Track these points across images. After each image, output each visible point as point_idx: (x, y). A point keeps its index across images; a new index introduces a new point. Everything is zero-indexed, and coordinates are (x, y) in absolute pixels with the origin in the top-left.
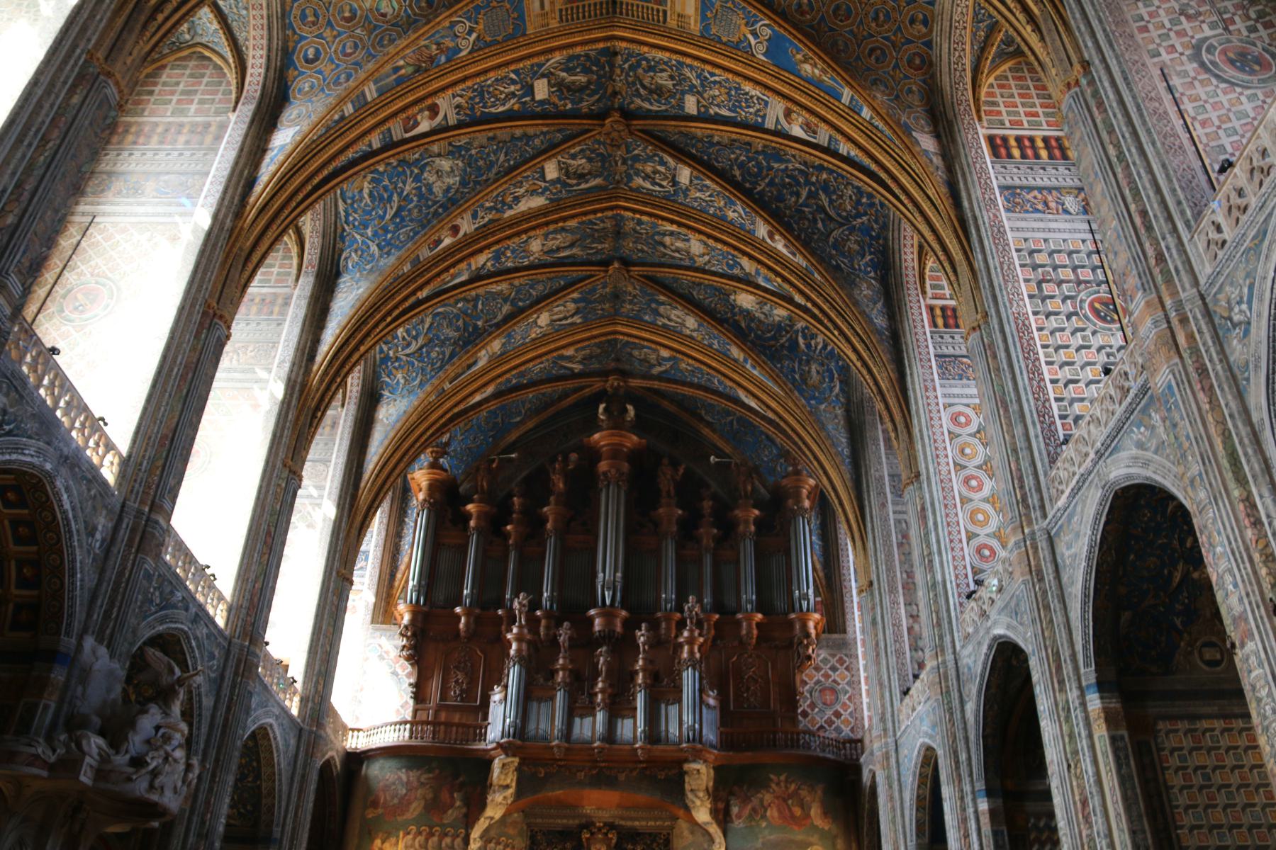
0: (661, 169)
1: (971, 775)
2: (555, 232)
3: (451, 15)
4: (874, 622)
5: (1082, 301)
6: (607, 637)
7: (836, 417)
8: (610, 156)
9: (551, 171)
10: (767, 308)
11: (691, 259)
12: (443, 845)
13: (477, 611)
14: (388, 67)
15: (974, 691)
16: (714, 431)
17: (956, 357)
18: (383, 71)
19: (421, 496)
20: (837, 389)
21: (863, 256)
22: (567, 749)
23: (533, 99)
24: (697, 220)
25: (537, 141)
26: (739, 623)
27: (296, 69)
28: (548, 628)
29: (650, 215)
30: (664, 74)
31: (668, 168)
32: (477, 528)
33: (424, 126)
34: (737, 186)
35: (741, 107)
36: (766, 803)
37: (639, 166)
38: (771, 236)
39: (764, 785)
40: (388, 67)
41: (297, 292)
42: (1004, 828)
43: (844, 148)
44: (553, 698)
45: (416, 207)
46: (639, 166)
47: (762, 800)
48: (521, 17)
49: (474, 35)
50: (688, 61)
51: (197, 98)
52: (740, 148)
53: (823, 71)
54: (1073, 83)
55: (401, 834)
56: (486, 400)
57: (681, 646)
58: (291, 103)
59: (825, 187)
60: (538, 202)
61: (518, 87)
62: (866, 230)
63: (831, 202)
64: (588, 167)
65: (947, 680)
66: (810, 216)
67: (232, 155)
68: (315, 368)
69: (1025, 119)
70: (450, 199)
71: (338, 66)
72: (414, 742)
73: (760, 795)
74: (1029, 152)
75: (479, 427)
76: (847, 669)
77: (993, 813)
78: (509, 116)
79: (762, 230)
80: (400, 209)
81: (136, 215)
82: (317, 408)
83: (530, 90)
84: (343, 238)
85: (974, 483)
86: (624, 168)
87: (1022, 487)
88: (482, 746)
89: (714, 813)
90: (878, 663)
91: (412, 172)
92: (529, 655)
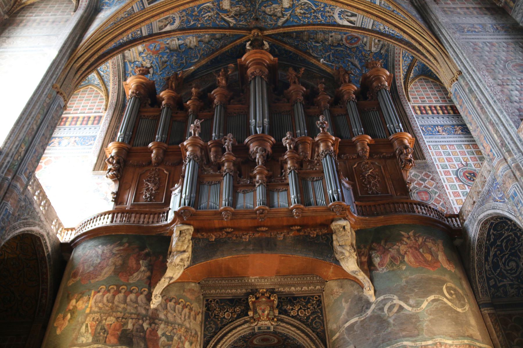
12: (128, 299)
22: (234, 214)
32: (166, 104)
36: (402, 252)
39: (399, 239)
44: (220, 182)
47: (398, 251)
55: (93, 292)
73: (395, 247)
75: (171, 66)
76: (432, 179)
89: (360, 264)
92: (201, 157)
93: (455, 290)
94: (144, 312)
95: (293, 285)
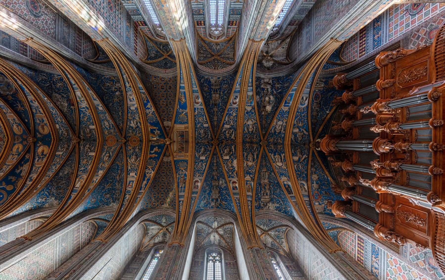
0: (227, 132)
8: (225, 144)
9: (228, 158)
23: (204, 160)
30: (200, 131)
37: (228, 137)
48: (184, 160)
49: (184, 170)
60: (235, 162)
64: (227, 149)
83: (202, 160)
86: (229, 141)
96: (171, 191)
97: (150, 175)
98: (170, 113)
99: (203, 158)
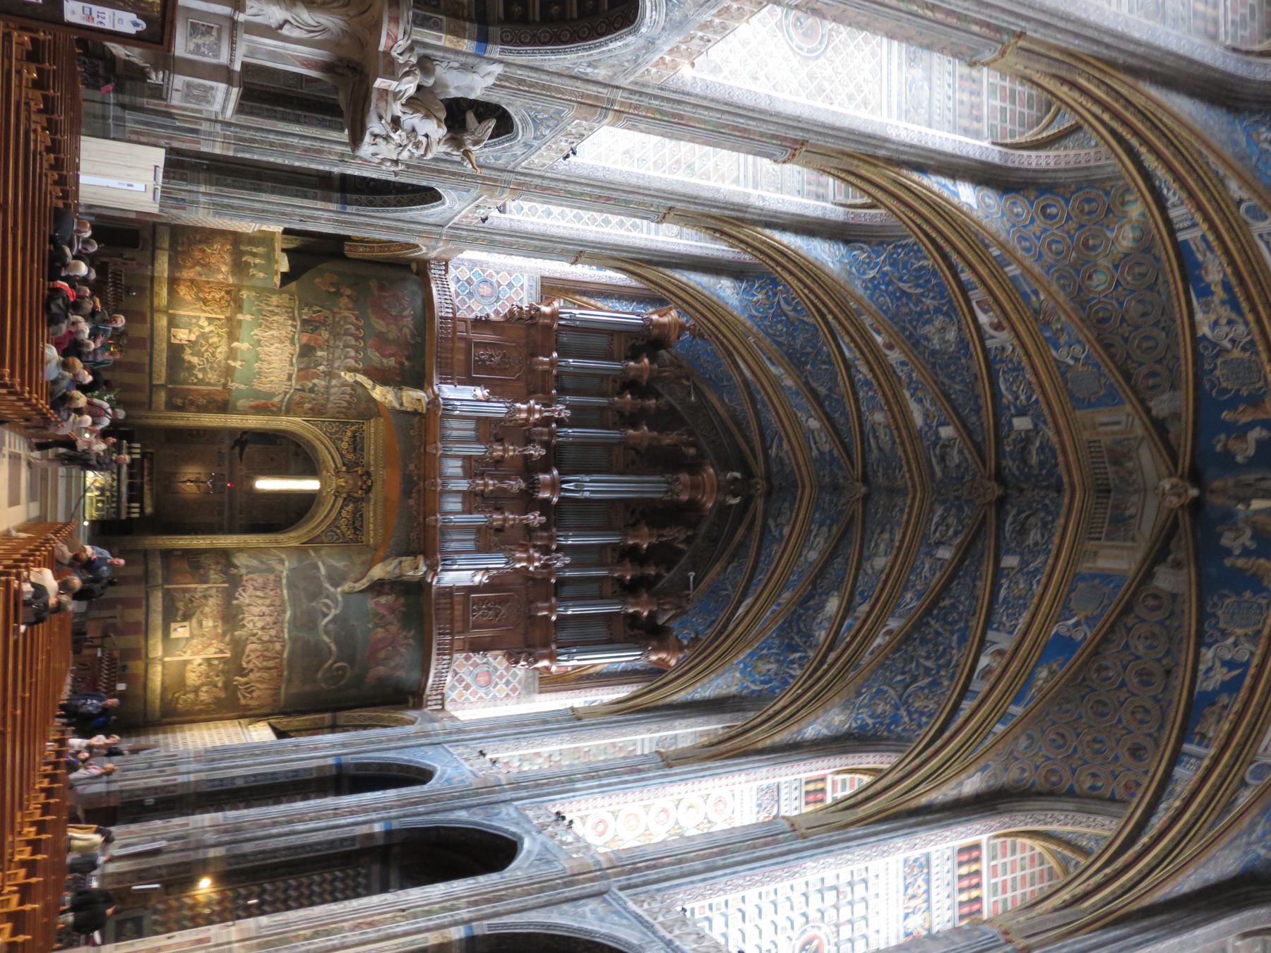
0: (951, 532)
1: (405, 816)
2: (892, 435)
3: (1089, 341)
4: (545, 722)
5: (819, 928)
6: (533, 486)
7: (729, 687)
9: (946, 432)
10: (826, 625)
11: (869, 558)
13: (555, 372)
14: (1037, 286)
15: (477, 819)
16: (719, 574)
17: (778, 801)
18: (1032, 281)
19: (655, 317)
20: (754, 687)
21: (871, 717)
23: (1013, 416)
24: (903, 564)
25: (974, 419)
26: (547, 600)
27: (1036, 198)
28: (542, 434)
29: (908, 522)
30: (1039, 537)
31: (951, 538)
33: (983, 318)
34: (935, 603)
35: (1007, 608)
37: (953, 511)
38: (889, 632)
40: (1037, 286)
41: (829, 206)
42: (357, 847)
43: (967, 705)
44: (478, 440)
45: (911, 311)
46: (953, 511)
48: (1090, 405)
49: (1071, 362)
50: (1050, 561)
51: (1008, 105)
52: (971, 605)
53: (1040, 689)
54: (1009, 937)
56: (741, 373)
57: (526, 551)
58: (1001, 197)
59: (935, 684)
60: (918, 419)
61: (1024, 402)
62: (896, 720)
63: (922, 688)
65: (488, 793)
66: (907, 669)
67: (948, 148)
68: (759, 229)
69: (999, 879)
70: (918, 341)
71: (1039, 238)
72: (437, 320)
74: (965, 883)
75: (719, 366)
76: (508, 695)
77: (370, 836)
78: (996, 395)
79: (893, 624)
80: (908, 295)
81: (889, 63)
82: (723, 233)
83: (1021, 413)
84: (881, 244)
85: (663, 816)
87: (648, 868)
88: (435, 381)
90: (508, 727)
91: (944, 305)
93: (343, 676)
94: (336, 365)
95: (375, 515)
96: (1126, 255)
97: (1213, 317)
98: (1157, 630)
99: (1022, 424)
